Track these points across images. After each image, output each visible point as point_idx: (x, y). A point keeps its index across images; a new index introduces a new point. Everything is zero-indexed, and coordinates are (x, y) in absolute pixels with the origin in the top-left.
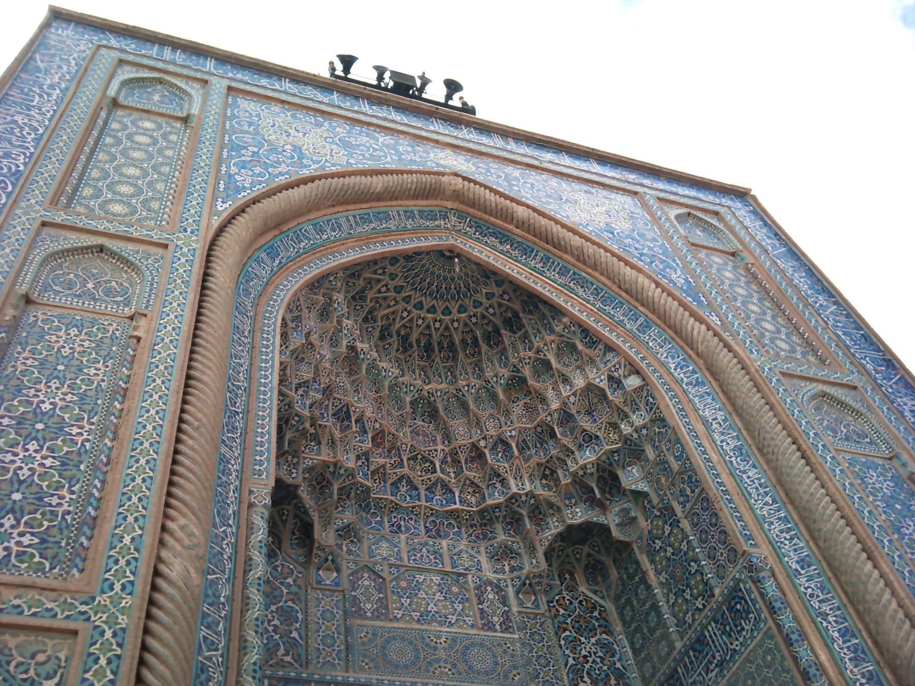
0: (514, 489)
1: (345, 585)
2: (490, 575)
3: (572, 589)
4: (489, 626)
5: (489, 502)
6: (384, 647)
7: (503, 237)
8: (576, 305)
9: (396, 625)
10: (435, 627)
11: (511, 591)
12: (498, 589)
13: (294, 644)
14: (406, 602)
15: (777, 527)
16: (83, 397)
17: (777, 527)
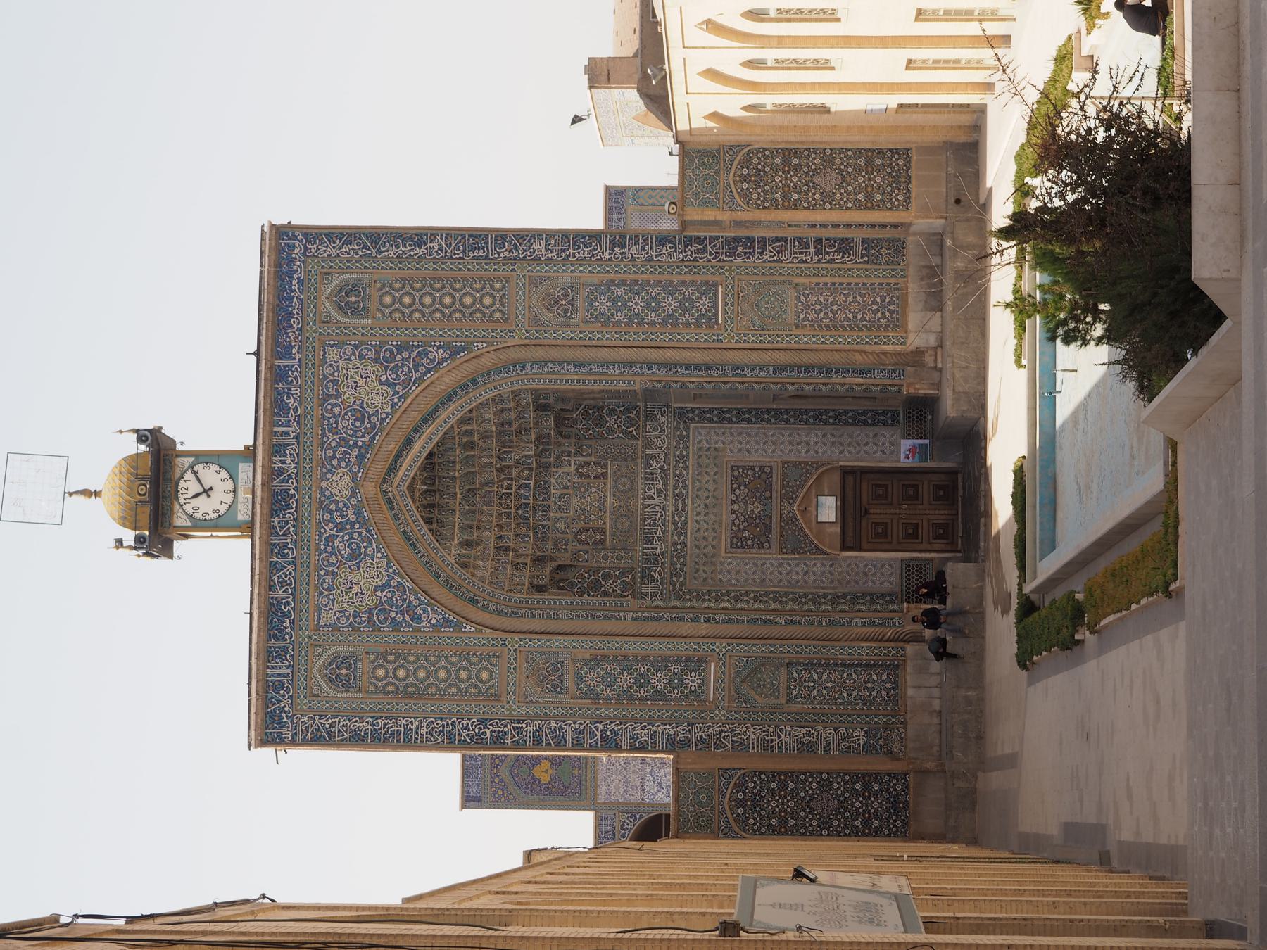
0: (532, 453)
1: (586, 547)
2: (573, 469)
3: (576, 422)
4: (604, 476)
5: (534, 466)
7: (399, 456)
8: (449, 416)
10: (608, 504)
11: (582, 459)
12: (581, 466)
13: (622, 575)
14: (593, 517)
15: (627, 370)
16: (624, 670)
17: (627, 370)
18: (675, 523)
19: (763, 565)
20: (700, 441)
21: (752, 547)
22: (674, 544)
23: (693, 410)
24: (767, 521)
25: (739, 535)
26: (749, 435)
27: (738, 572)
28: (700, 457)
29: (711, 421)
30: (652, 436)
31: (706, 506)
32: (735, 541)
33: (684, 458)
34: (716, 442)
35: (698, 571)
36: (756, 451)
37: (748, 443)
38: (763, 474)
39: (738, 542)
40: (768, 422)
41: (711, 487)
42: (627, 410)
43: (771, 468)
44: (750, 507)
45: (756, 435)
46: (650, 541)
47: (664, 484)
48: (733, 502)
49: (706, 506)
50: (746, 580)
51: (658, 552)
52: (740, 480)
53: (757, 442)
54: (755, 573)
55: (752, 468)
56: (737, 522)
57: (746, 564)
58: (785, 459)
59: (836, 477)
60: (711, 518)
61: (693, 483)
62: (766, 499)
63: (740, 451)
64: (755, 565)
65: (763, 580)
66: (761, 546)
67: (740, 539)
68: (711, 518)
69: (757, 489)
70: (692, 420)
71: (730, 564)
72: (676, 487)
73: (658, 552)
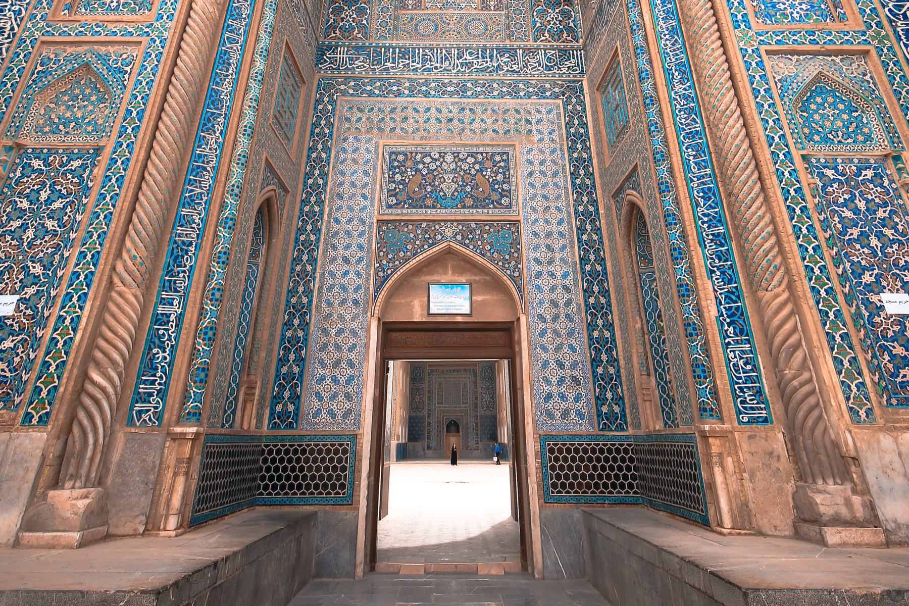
6: (416, 25)
9: (425, 12)
10: (451, 11)
18: (427, 83)
19: (364, 197)
20: (539, 112)
21: (391, 180)
22: (399, 82)
23: (582, 103)
24: (429, 202)
25: (409, 163)
26: (555, 174)
27: (355, 161)
28: (517, 111)
29: (569, 125)
30: (541, 56)
31: (451, 120)
32: (401, 158)
33: (514, 93)
34: (539, 131)
35: (361, 110)
36: (531, 184)
37: (543, 173)
38: (500, 194)
39: (397, 163)
40: (578, 203)
41: (476, 125)
42: (570, 31)
43: (509, 206)
44: (449, 177)
45: (555, 184)
46: (403, 55)
47: (477, 70)
48: (456, 155)
49: (451, 120)
50: (343, 173)
51: (389, 65)
52: (489, 164)
53: (544, 186)
54: (353, 185)
55: (507, 180)
56: (427, 160)
57: (366, 173)
58: (524, 228)
59: (498, 315)
60: (433, 126)
61: (482, 104)
62: (462, 201)
63: (530, 162)
64: (365, 185)
65: (340, 197)
66: (392, 193)
67: (402, 164)
68: (433, 126)
69: (475, 187)
70: (567, 103)
71: (367, 150)
72: (476, 83)
73: (389, 65)
